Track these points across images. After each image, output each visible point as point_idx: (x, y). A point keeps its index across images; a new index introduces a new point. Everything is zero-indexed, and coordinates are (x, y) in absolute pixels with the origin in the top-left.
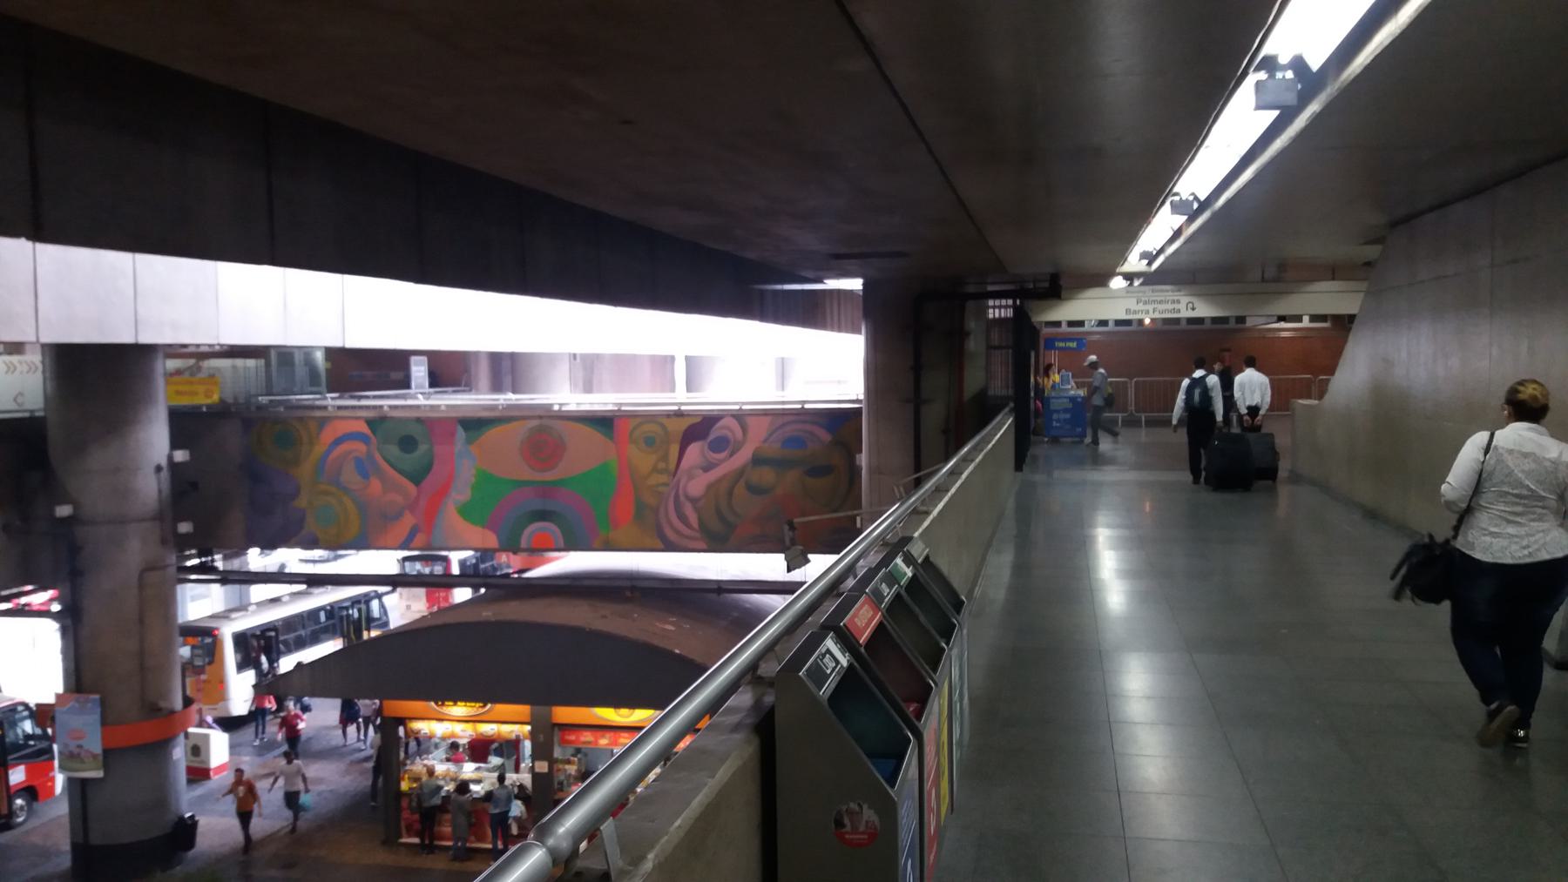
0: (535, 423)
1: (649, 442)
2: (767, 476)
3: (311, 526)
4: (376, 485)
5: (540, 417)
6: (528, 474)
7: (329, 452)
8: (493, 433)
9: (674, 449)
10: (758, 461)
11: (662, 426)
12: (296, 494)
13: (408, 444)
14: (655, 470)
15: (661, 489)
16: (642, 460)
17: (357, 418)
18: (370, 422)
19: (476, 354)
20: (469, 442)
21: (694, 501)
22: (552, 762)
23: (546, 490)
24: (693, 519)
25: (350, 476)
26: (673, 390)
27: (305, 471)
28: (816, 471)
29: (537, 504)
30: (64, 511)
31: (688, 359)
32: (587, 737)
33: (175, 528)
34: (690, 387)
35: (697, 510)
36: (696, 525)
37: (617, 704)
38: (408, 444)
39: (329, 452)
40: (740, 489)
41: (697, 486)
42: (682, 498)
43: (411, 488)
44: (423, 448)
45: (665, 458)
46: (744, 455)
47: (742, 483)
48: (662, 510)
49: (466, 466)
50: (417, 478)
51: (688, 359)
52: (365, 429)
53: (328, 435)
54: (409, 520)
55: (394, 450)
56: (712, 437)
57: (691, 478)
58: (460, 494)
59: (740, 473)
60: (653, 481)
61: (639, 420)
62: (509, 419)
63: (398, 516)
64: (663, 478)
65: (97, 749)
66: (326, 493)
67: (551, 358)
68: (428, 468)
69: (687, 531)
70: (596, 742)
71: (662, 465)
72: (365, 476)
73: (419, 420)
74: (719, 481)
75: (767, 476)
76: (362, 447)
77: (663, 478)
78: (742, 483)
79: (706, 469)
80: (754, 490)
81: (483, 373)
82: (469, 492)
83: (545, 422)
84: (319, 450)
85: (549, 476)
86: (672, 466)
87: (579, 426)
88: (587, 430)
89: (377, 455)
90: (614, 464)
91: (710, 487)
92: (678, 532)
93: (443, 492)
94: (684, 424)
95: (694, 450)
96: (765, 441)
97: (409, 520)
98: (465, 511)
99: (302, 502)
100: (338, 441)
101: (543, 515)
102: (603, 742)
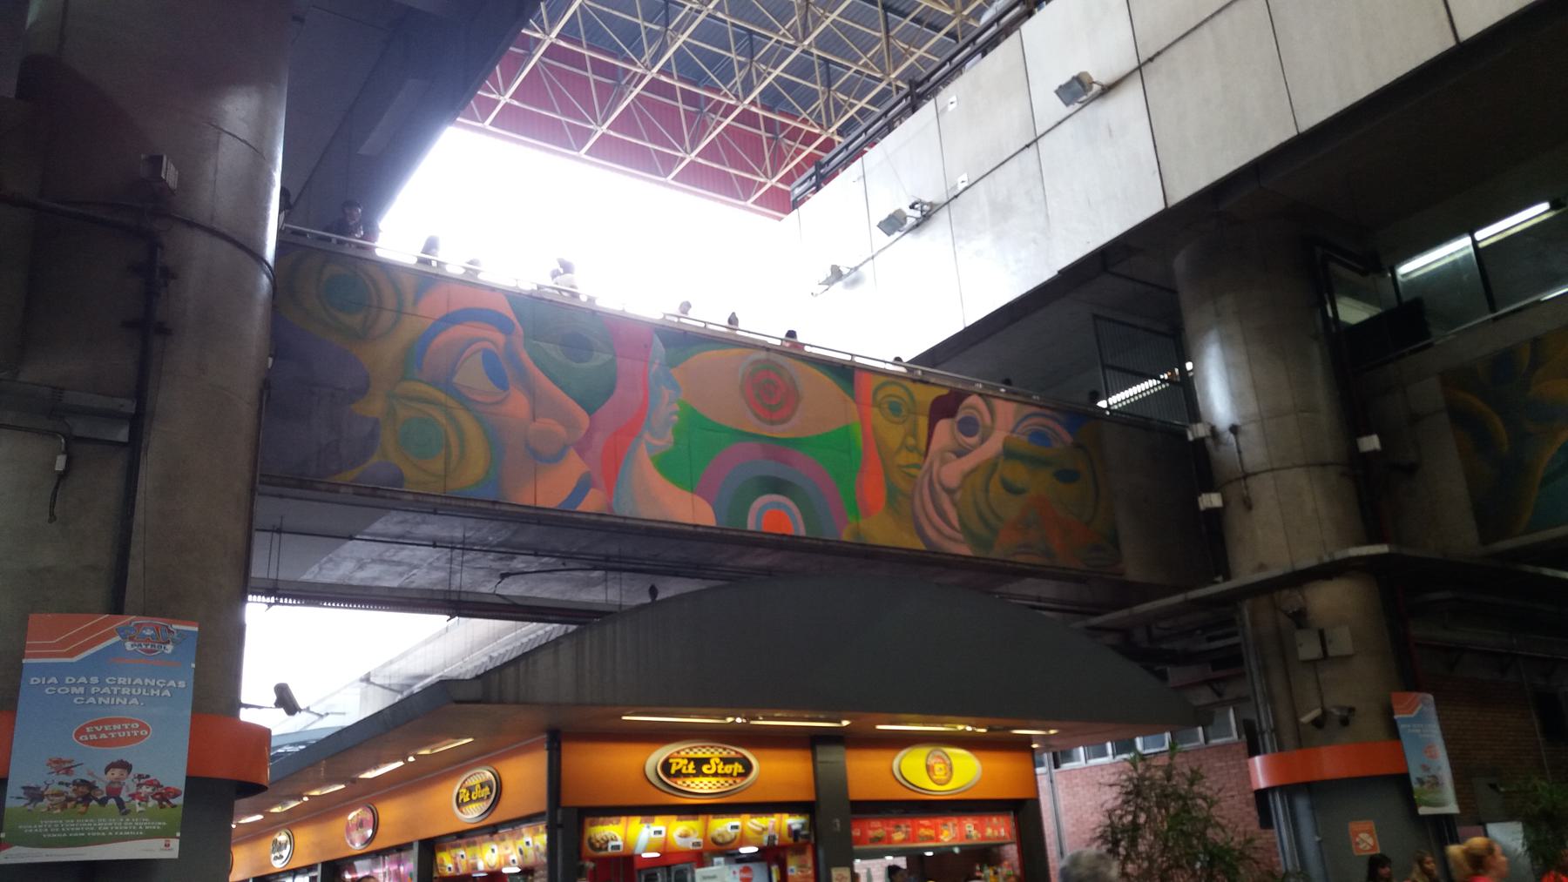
0: (763, 355)
1: (895, 409)
2: (1019, 474)
6: (753, 425)
9: (923, 422)
10: (1009, 453)
11: (906, 389)
12: (362, 390)
14: (904, 445)
15: (913, 471)
16: (893, 434)
21: (950, 492)
23: (778, 449)
24: (952, 515)
29: (771, 469)
35: (955, 504)
36: (956, 524)
40: (995, 485)
41: (952, 472)
42: (938, 487)
45: (915, 436)
46: (994, 445)
47: (996, 477)
48: (917, 503)
56: (959, 416)
57: (944, 462)
59: (992, 466)
63: (557, 458)
64: (914, 458)
65: (175, 777)
70: (890, 841)
71: (911, 441)
72: (500, 380)
74: (973, 471)
76: (500, 338)
77: (914, 458)
79: (960, 453)
82: (670, 436)
85: (780, 431)
87: (814, 372)
90: (857, 428)
91: (967, 475)
95: (943, 426)
96: (1013, 431)
98: (665, 464)
99: (374, 407)
101: (776, 485)
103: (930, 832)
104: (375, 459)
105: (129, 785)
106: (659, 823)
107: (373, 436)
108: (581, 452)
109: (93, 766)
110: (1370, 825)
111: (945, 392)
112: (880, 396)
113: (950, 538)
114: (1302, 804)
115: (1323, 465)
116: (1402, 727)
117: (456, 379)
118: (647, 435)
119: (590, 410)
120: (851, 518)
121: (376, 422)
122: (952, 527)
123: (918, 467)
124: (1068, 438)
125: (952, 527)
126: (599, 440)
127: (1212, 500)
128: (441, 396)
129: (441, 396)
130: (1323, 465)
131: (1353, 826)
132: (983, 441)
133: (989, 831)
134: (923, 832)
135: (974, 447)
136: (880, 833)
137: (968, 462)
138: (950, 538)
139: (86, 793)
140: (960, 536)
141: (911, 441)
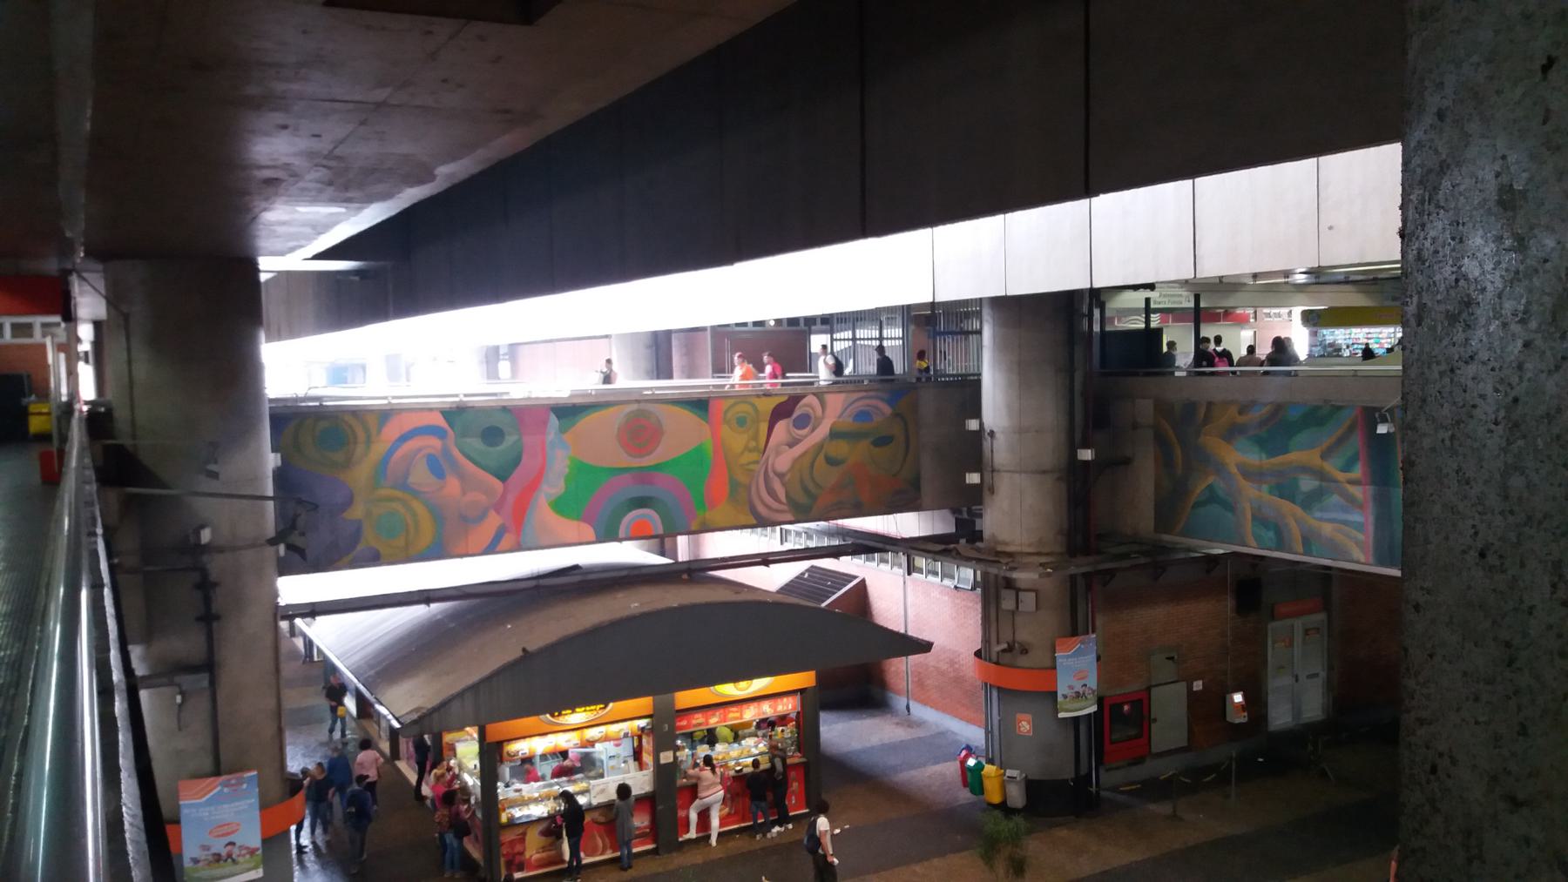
0: (635, 407)
1: (741, 422)
2: (841, 449)
3: (369, 539)
4: (453, 485)
5: (638, 401)
7: (390, 452)
9: (764, 427)
10: (835, 435)
11: (753, 405)
12: (349, 502)
13: (492, 435)
14: (747, 449)
16: (736, 441)
20: (562, 430)
21: (781, 476)
23: (644, 476)
25: (420, 476)
27: (360, 475)
28: (882, 441)
32: (698, 718)
35: (784, 484)
36: (784, 499)
37: (735, 678)
39: (390, 452)
41: (783, 462)
42: (771, 474)
43: (497, 485)
44: (510, 440)
45: (755, 438)
46: (823, 431)
48: (753, 489)
50: (503, 475)
52: (441, 421)
53: (392, 431)
54: (494, 521)
55: (476, 443)
56: (795, 415)
57: (778, 453)
58: (553, 486)
59: (820, 447)
62: (607, 405)
63: (482, 516)
64: (755, 456)
65: (255, 841)
66: (391, 499)
68: (516, 462)
69: (775, 505)
71: (753, 444)
73: (505, 409)
75: (841, 449)
76: (434, 443)
77: (755, 456)
78: (821, 457)
79: (791, 445)
80: (832, 462)
82: (562, 483)
85: (647, 461)
87: (676, 409)
88: (687, 415)
90: (709, 445)
91: (795, 461)
92: (766, 506)
93: (533, 486)
95: (781, 426)
98: (559, 506)
99: (357, 512)
100: (404, 438)
101: (641, 502)
104: (360, 547)
105: (236, 851)
106: (551, 737)
108: (498, 511)
109: (219, 846)
110: (1029, 717)
111: (784, 399)
112: (729, 415)
113: (778, 511)
114: (995, 693)
115: (1044, 472)
116: (1059, 661)
117: (411, 480)
120: (700, 513)
121: (359, 522)
122: (780, 502)
124: (887, 410)
125: (780, 502)
126: (511, 499)
127: (973, 478)
130: (1044, 472)
131: (1019, 716)
132: (813, 430)
136: (701, 720)
137: (799, 450)
138: (778, 511)
139: (218, 858)
141: (753, 444)
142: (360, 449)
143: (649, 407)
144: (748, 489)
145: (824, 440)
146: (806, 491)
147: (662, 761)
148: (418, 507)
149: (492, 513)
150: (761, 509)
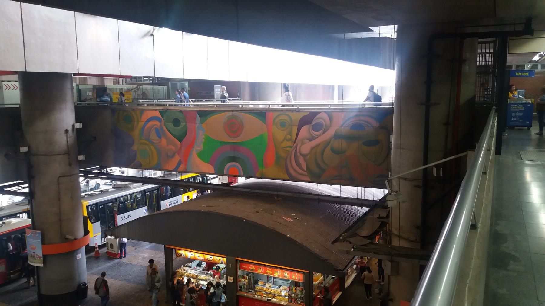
0: (231, 114)
1: (283, 124)
3: (139, 159)
8: (212, 119)
9: (295, 129)
10: (337, 136)
11: (288, 116)
12: (133, 144)
13: (176, 122)
14: (285, 139)
15: (288, 149)
16: (280, 134)
17: (156, 110)
18: (161, 112)
19: (244, 83)
20: (202, 123)
21: (304, 156)
22: (236, 277)
23: (235, 147)
25: (153, 136)
26: (333, 99)
27: (136, 133)
29: (232, 154)
30: (24, 149)
31: (339, 87)
33: (77, 158)
34: (340, 97)
35: (305, 160)
38: (176, 122)
40: (328, 151)
41: (306, 148)
42: (299, 154)
44: (183, 124)
45: (290, 133)
46: (330, 133)
47: (329, 147)
48: (288, 161)
49: (201, 133)
50: (180, 139)
51: (339, 87)
52: (158, 114)
54: (177, 158)
55: (171, 125)
56: (313, 123)
57: (303, 143)
58: (198, 147)
59: (328, 143)
60: (284, 145)
61: (279, 113)
62: (220, 112)
63: (173, 156)
67: (274, 85)
68: (185, 134)
70: (256, 271)
71: (289, 137)
72: (159, 136)
74: (317, 146)
76: (158, 123)
77: (289, 144)
79: (310, 140)
80: (333, 151)
81: (246, 92)
83: (235, 113)
84: (141, 124)
85: (236, 140)
86: (294, 138)
88: (253, 118)
89: (165, 128)
90: (266, 135)
91: (312, 149)
94: (300, 116)
95: (305, 129)
97: (177, 158)
98: (201, 155)
99: (135, 147)
100: (148, 121)
101: (233, 159)
102: (259, 271)
103: (271, 272)
107: (136, 155)
108: (179, 154)
117: (150, 137)
118: (195, 147)
119: (181, 141)
120: (260, 169)
122: (303, 170)
123: (291, 147)
125: (303, 170)
128: (147, 143)
129: (147, 143)
132: (324, 132)
133: (293, 277)
134: (268, 271)
135: (319, 136)
136: (253, 268)
140: (306, 173)
142: (136, 123)
143: (235, 113)
144: (286, 160)
145: (331, 139)
146: (318, 165)
147: (229, 280)
148: (152, 147)
149: (177, 154)
150: (292, 172)
